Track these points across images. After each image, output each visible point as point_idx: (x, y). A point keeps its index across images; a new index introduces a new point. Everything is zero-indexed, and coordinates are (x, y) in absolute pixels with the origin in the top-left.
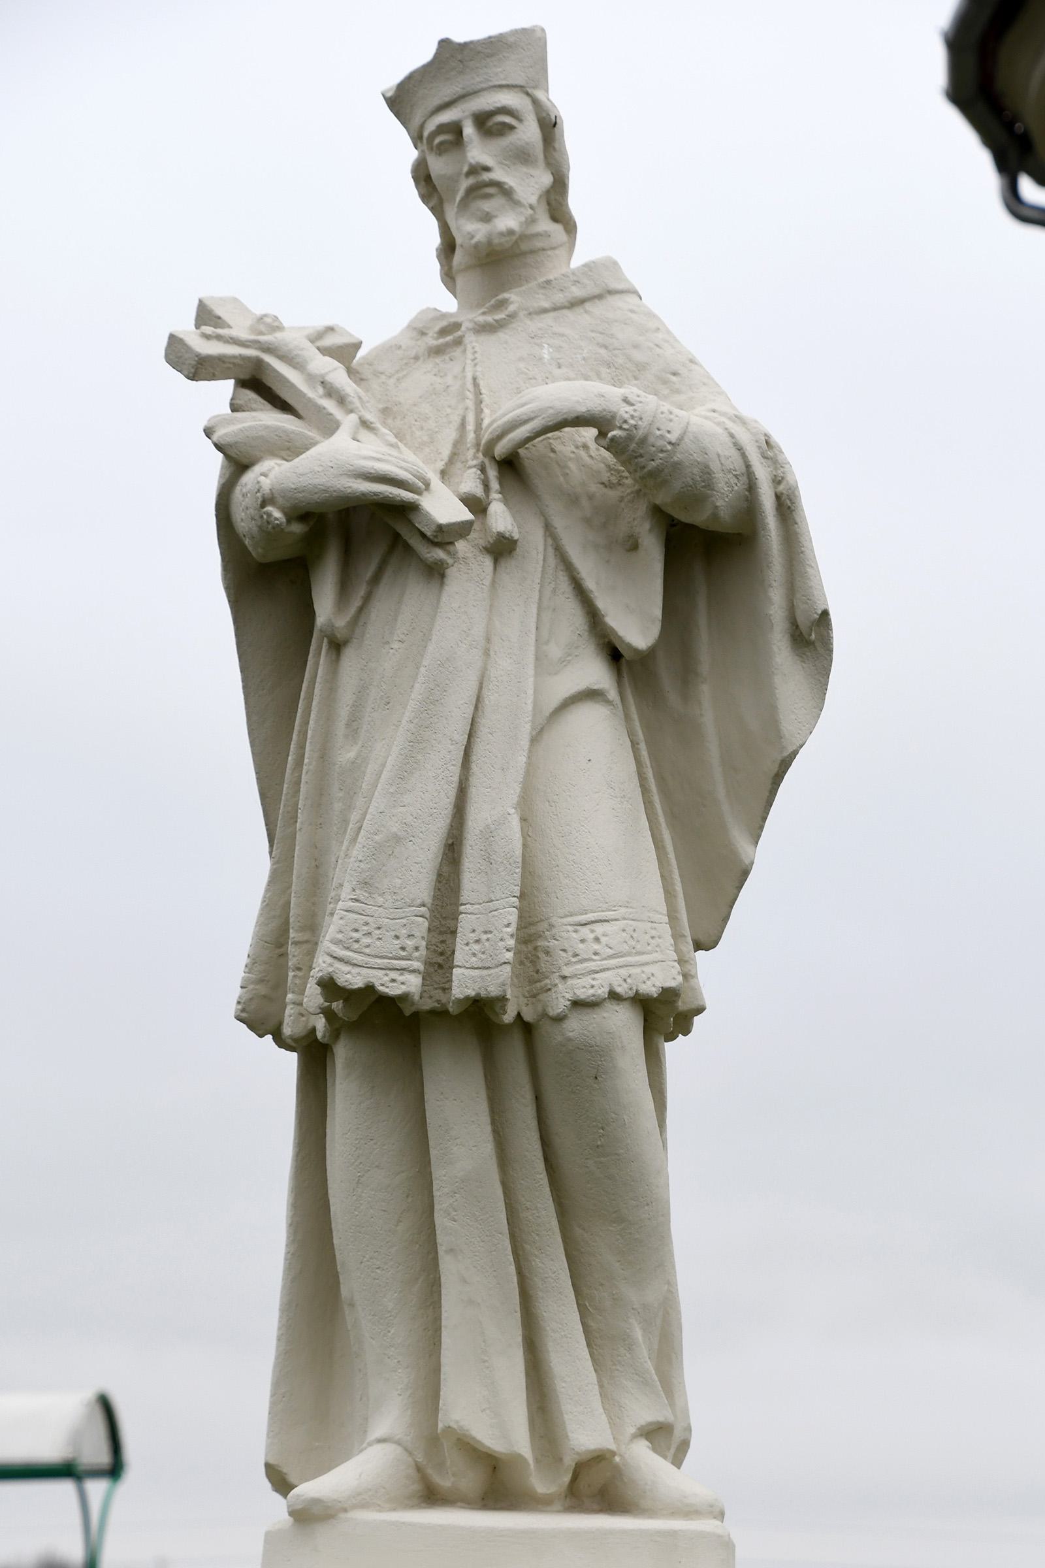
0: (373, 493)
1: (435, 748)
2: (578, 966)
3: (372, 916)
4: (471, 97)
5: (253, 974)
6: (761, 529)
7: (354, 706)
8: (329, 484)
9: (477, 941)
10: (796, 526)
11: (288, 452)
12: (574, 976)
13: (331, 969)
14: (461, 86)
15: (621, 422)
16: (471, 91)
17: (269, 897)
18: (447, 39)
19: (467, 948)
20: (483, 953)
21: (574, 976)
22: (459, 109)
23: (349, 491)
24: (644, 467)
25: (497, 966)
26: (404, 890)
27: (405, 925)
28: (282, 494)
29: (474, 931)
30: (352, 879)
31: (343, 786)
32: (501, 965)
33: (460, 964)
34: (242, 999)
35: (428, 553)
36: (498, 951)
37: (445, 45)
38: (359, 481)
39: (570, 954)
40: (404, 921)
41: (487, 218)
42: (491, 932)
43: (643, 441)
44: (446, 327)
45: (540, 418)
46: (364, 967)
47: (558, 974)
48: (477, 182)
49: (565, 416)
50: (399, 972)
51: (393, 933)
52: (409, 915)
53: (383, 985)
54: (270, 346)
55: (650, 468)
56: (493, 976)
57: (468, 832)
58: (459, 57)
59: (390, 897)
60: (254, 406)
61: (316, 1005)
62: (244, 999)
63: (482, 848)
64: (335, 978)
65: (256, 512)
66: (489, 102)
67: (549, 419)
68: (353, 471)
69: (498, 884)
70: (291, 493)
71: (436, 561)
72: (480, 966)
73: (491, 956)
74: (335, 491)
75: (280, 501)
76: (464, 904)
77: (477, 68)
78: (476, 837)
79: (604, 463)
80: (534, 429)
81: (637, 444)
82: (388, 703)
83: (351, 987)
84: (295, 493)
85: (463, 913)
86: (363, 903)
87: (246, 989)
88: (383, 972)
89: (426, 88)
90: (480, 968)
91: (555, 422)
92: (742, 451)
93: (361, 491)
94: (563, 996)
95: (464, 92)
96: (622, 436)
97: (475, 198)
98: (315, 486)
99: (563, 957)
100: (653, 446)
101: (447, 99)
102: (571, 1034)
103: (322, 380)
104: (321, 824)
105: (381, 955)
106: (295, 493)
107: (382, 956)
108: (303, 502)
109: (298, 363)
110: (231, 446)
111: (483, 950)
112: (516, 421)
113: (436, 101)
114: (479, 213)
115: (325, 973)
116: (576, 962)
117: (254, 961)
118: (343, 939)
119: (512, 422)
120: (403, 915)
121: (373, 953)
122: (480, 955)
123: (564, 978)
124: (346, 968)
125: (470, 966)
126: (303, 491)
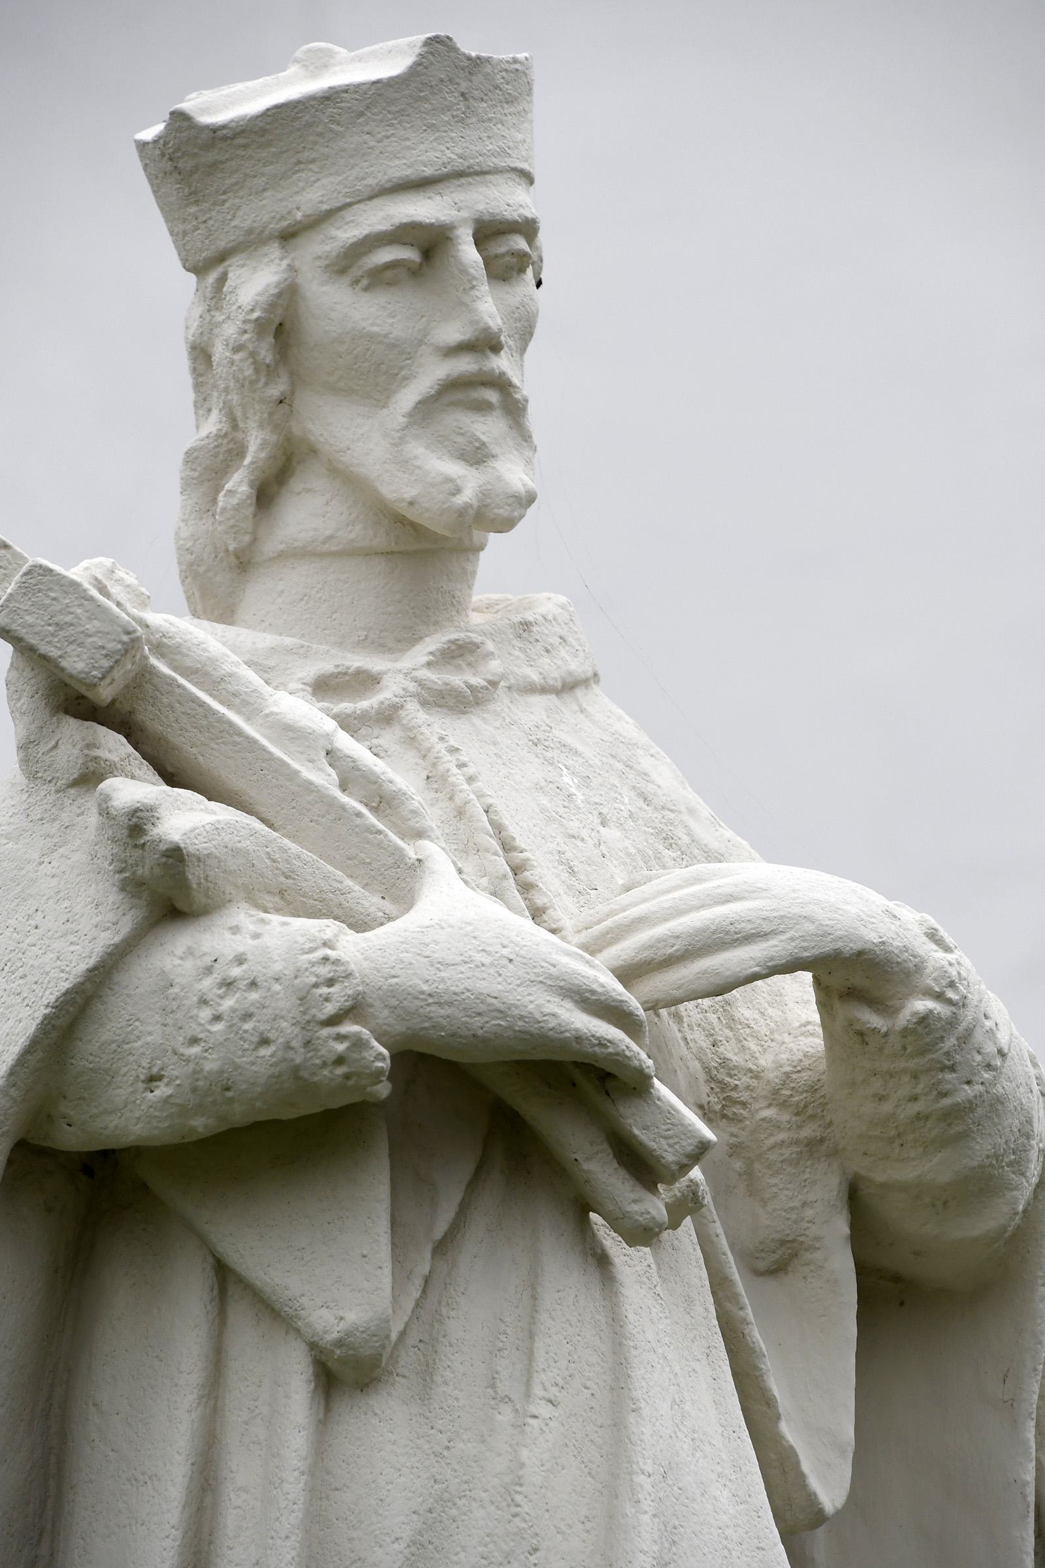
0: (598, 1038)
8: (511, 999)
11: (277, 899)
14: (458, 150)
15: (944, 982)
24: (945, 1095)
28: (394, 1002)
37: (438, 46)
38: (569, 1004)
45: (783, 937)
48: (481, 369)
49: (840, 944)
58: (464, 86)
66: (510, 202)
67: (804, 944)
68: (557, 978)
74: (522, 1017)
80: (772, 959)
81: (958, 1039)
84: (429, 1005)
91: (816, 952)
93: (576, 1030)
97: (452, 404)
98: (481, 998)
100: (979, 1052)
101: (428, 171)
106: (429, 1005)
108: (443, 1028)
112: (727, 933)
114: (460, 439)
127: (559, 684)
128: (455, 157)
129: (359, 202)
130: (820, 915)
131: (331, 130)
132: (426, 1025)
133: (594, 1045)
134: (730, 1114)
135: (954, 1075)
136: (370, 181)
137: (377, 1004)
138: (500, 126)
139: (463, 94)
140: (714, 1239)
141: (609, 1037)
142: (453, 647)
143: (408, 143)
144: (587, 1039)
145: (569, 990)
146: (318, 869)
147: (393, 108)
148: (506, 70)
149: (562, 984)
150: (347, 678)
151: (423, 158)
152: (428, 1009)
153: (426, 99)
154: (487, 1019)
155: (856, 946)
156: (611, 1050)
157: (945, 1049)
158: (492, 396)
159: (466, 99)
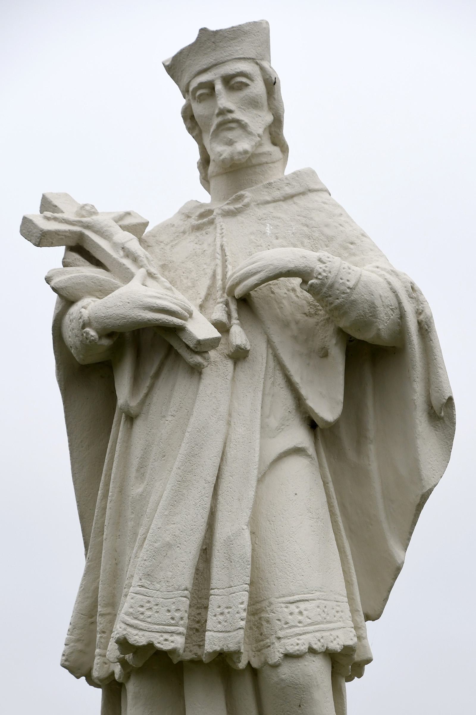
0: (155, 319)
1: (195, 486)
2: (288, 631)
3: (153, 597)
4: (219, 65)
5: (73, 636)
6: (408, 344)
7: (141, 458)
8: (127, 314)
9: (222, 614)
10: (431, 342)
11: (100, 293)
12: (286, 637)
13: (125, 632)
14: (214, 58)
15: (317, 274)
16: (221, 62)
17: (84, 584)
18: (205, 28)
19: (215, 618)
20: (226, 621)
21: (286, 637)
22: (212, 73)
23: (140, 318)
24: (332, 303)
25: (235, 630)
26: (174, 579)
27: (174, 603)
28: (96, 320)
29: (219, 607)
30: (140, 572)
31: (134, 511)
32: (237, 629)
33: (210, 629)
34: (66, 653)
35: (191, 358)
36: (236, 620)
37: (203, 31)
38: (146, 311)
39: (283, 622)
40: (174, 600)
41: (230, 143)
42: (230, 608)
43: (331, 286)
44: (204, 212)
45: (264, 271)
46: (147, 631)
47: (275, 636)
48: (224, 119)
49: (281, 270)
50: (170, 634)
51: (166, 608)
52: (176, 596)
53: (159, 643)
54: (89, 225)
55: (335, 304)
56: (231, 637)
57: (216, 541)
58: (213, 40)
59: (164, 584)
60: (78, 263)
61: (115, 656)
62: (67, 652)
63: (225, 551)
64: (127, 638)
65: (79, 331)
66: (232, 69)
67: (270, 272)
68: (142, 305)
69: (235, 576)
70: (102, 320)
71: (196, 364)
72: (224, 630)
73: (231, 623)
74: (130, 318)
75: (95, 324)
76: (214, 589)
77: (225, 47)
78: (221, 545)
79: (306, 300)
80: (261, 278)
81: (327, 288)
82: (165, 456)
83: (138, 644)
84: (105, 320)
85: (212, 595)
86: (146, 588)
87: (68, 646)
88: (160, 634)
89: (191, 60)
90: (224, 632)
91: (274, 274)
92: (396, 293)
93: (148, 318)
94: (278, 651)
95: (214, 62)
96: (318, 283)
97: (223, 130)
98: (118, 315)
99: (278, 624)
100: (338, 290)
101: (205, 67)
102: (283, 676)
103: (123, 247)
104: (119, 536)
105: (158, 623)
106: (105, 320)
107: (159, 624)
108: (110, 325)
109: (107, 236)
110: (63, 289)
111: (225, 620)
112: (249, 273)
113: (198, 68)
114: (225, 139)
115: (121, 635)
116: (287, 628)
117: (74, 627)
118: (134, 612)
119: (246, 274)
120: (173, 596)
121: (153, 622)
122: (223, 623)
123: (279, 638)
124: (135, 632)
125: (217, 630)
126: (110, 318)
127: (282, 198)
128: (212, 60)
129: (192, 79)
130: (276, 263)
131: (183, 61)
132: (105, 325)
133: (155, 321)
134: (318, 314)
135: (331, 298)
136: (193, 73)
137: (93, 322)
138: (229, 48)
139: (213, 42)
140: (278, 355)
141: (159, 318)
142: (237, 197)
143: (200, 60)
144: (152, 320)
145: (146, 308)
146: (110, 282)
147: (195, 51)
148: (229, 31)
149: (144, 306)
150: (207, 212)
151: (204, 63)
152: (105, 321)
153: (202, 47)
154: (120, 320)
155: (286, 270)
156: (161, 322)
157: (323, 292)
158: (233, 125)
159: (214, 43)
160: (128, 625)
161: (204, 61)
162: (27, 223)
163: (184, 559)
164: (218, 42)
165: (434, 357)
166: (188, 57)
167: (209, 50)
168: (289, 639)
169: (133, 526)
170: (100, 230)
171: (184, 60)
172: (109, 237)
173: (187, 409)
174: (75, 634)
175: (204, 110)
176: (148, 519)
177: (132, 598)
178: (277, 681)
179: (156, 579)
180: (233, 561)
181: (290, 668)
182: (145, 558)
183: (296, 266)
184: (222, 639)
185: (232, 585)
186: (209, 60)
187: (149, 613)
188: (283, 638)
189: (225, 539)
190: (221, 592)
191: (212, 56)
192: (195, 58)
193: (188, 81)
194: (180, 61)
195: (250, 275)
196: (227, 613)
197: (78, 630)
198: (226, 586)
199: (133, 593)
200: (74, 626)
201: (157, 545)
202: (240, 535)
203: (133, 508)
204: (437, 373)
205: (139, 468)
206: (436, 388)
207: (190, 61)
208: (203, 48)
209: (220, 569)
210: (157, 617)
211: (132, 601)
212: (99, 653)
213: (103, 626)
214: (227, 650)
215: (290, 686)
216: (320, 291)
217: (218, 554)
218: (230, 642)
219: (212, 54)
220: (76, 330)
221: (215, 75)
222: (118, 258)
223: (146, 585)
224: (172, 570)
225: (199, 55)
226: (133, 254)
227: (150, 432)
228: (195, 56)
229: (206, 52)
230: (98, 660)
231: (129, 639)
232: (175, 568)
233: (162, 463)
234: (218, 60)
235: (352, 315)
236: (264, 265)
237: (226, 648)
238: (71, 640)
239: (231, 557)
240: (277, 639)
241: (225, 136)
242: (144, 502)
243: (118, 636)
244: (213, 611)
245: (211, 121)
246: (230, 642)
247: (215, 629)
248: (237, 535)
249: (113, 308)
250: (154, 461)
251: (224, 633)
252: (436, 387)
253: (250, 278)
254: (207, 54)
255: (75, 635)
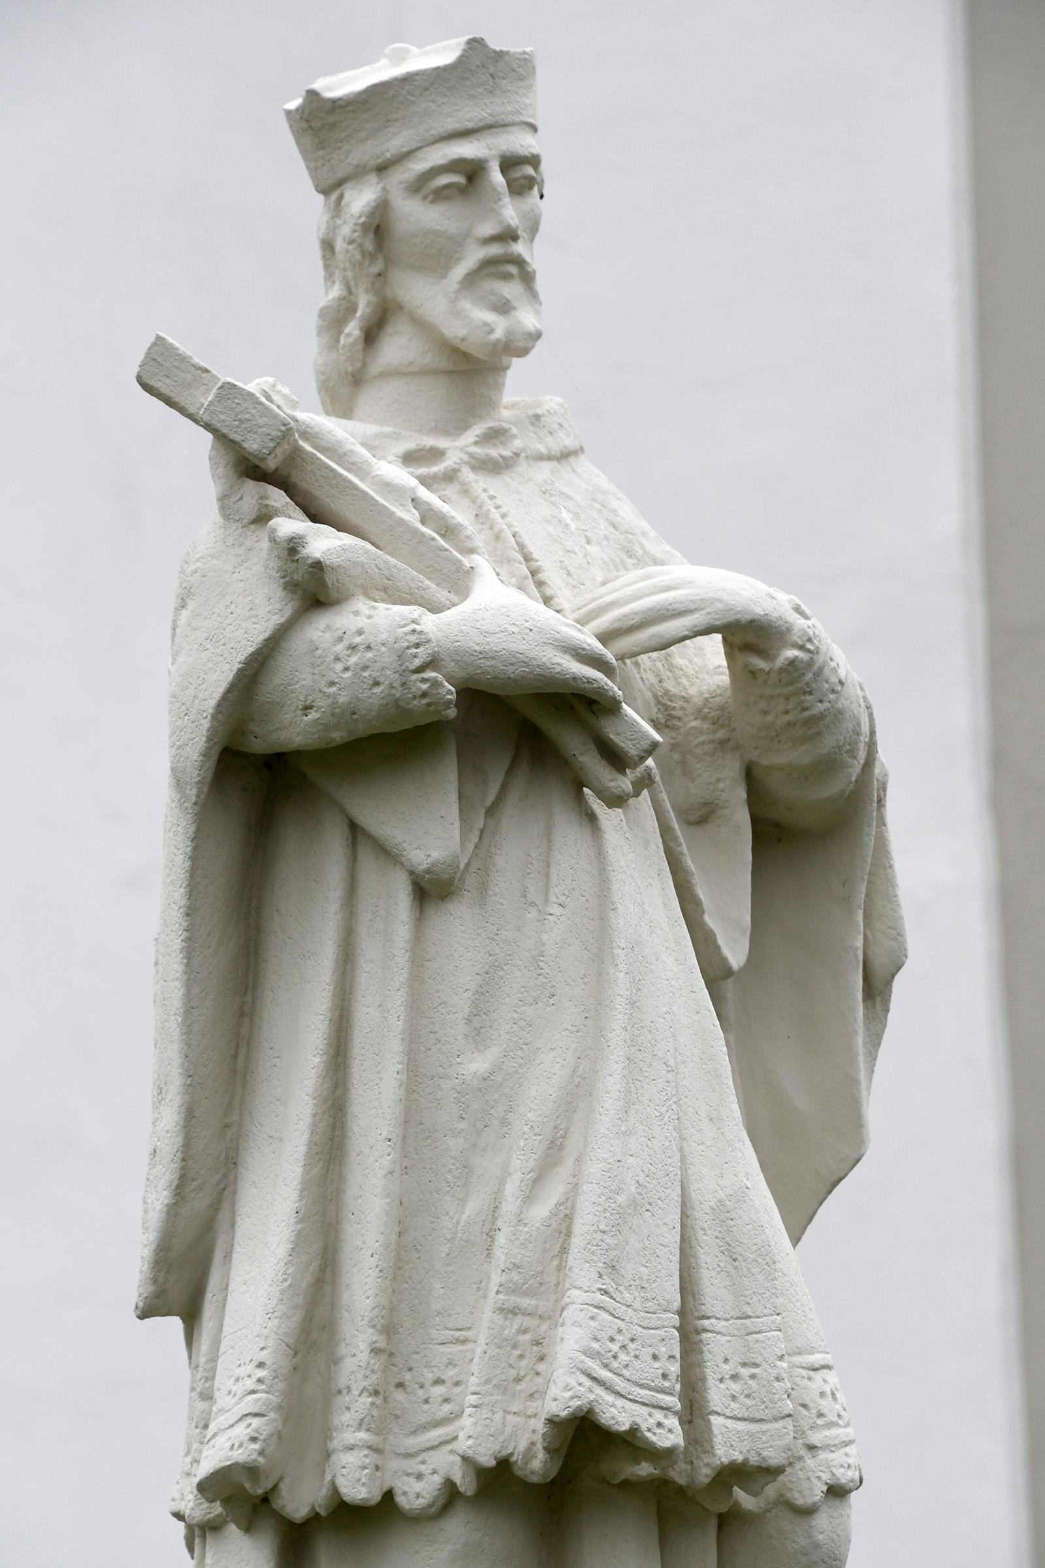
0: (587, 678)
1: (646, 1074)
2: (827, 1433)
3: (623, 1320)
4: (497, 130)
5: (273, 1394)
6: (866, 824)
7: (477, 992)
8: (532, 654)
9: (735, 1377)
10: (883, 827)
11: (382, 594)
12: (827, 1447)
13: (592, 1397)
14: (489, 111)
15: (805, 639)
16: (501, 123)
17: (293, 1272)
18: (482, 39)
19: (722, 1386)
20: (748, 1396)
21: (827, 1447)
23: (558, 669)
24: (806, 709)
25: (776, 1419)
26: (654, 1285)
27: (663, 1339)
28: (458, 658)
29: (726, 1361)
32: (783, 1418)
33: (719, 1411)
34: (261, 1434)
36: (777, 1396)
37: (476, 45)
38: (568, 657)
39: (814, 1411)
40: (661, 1332)
41: (504, 308)
42: (756, 1365)
43: (819, 673)
45: (703, 612)
46: (626, 1398)
47: (801, 1441)
48: (505, 252)
49: (739, 616)
50: (663, 1412)
51: (650, 1350)
53: (649, 1430)
54: (308, 429)
55: (815, 712)
56: (769, 1434)
58: (492, 69)
59: (637, 1295)
60: (292, 514)
61: (491, 1452)
63: (717, 1234)
64: (597, 1411)
65: (397, 676)
66: (522, 144)
67: (716, 617)
68: (561, 641)
69: (754, 1292)
71: (622, 794)
72: (746, 1416)
73: (764, 1402)
74: (538, 666)
75: (451, 666)
76: (708, 1318)
77: (509, 91)
78: (707, 1217)
80: (696, 626)
81: (814, 674)
84: (479, 659)
85: (708, 1331)
86: (611, 1297)
87: (264, 1419)
88: (648, 1410)
91: (724, 621)
92: (870, 711)
93: (573, 673)
97: (489, 275)
98: (513, 654)
99: (805, 1416)
100: (827, 682)
101: (470, 125)
102: (820, 1537)
103: (413, 496)
104: (406, 1168)
105: (642, 1382)
106: (479, 659)
107: (642, 1384)
108: (489, 673)
110: (333, 569)
111: (746, 1392)
112: (668, 610)
114: (492, 298)
115: (585, 1401)
116: (823, 1425)
117: (274, 1374)
118: (601, 1350)
121: (633, 1378)
122: (742, 1399)
123: (811, 1448)
124: (610, 1398)
127: (559, 454)
128: (486, 115)
129: (427, 146)
130: (726, 597)
131: (408, 100)
132: (479, 671)
133: (585, 683)
134: (671, 725)
135: (811, 697)
136: (433, 132)
137: (447, 659)
138: (515, 95)
139: (491, 75)
140: (662, 802)
141: (594, 678)
142: (492, 432)
143: (457, 107)
144: (580, 678)
145: (567, 648)
146: (408, 574)
147: (447, 85)
148: (519, 59)
149: (563, 644)
150: (424, 452)
151: (467, 117)
152: (479, 661)
153: (468, 78)
154: (517, 667)
155: (749, 617)
156: (595, 686)
157: (806, 681)
158: (513, 270)
159: (493, 78)
160: (594, 1379)
161: (469, 112)
162: (235, 398)
163: (666, 1240)
164: (499, 78)
165: (889, 863)
166: (427, 93)
167: (480, 90)
168: (832, 1451)
169: (463, 1149)
170: (337, 447)
171: (410, 98)
172: (360, 469)
173: (584, 894)
174: (277, 1391)
175: (447, 222)
176: (538, 1138)
177: (592, 1318)
178: (805, 1548)
179: (622, 1279)
180: (740, 1258)
181: (831, 1520)
182: (602, 1227)
183: (767, 612)
184: (745, 1437)
185: (751, 1314)
186: (479, 113)
187: (623, 1357)
188: (820, 1448)
189: (712, 1204)
190: (724, 1326)
191: (485, 104)
192: (445, 100)
193: (413, 148)
194: (394, 97)
195: (668, 614)
196: (747, 1378)
197: (280, 1381)
198: (731, 1314)
199: (592, 1305)
200: (274, 1371)
201: (621, 1200)
202: (744, 1201)
203: (463, 1105)
204: (895, 897)
205: (472, 1015)
206: (890, 930)
207: (431, 104)
208: (469, 83)
209: (713, 1274)
210: (638, 1367)
211: (593, 1323)
212: (368, 1442)
213: (377, 1378)
214: (756, 1464)
215: (825, 1562)
216: (799, 678)
217: (705, 1237)
218: (767, 1445)
219: (485, 101)
220: (389, 672)
221: (490, 150)
222: (412, 520)
223: (611, 1290)
224: (647, 1262)
225: (457, 95)
226: (443, 519)
227: (497, 934)
228: (446, 96)
229: (473, 92)
230: (364, 1459)
231: (601, 1414)
232: (652, 1259)
233: (550, 1011)
234: (498, 118)
235: (826, 742)
236: (702, 597)
237: (756, 1458)
238: (270, 1404)
239: (734, 1248)
240: (806, 1450)
241: (493, 290)
242: (496, 1096)
243: (579, 1403)
244: (715, 1368)
245: (460, 249)
246: (767, 1445)
247: (728, 1412)
248: (739, 1201)
249: (499, 635)
250: (521, 1003)
251: (746, 1423)
252: (890, 928)
253: (668, 620)
254: (476, 99)
255: (276, 1394)
